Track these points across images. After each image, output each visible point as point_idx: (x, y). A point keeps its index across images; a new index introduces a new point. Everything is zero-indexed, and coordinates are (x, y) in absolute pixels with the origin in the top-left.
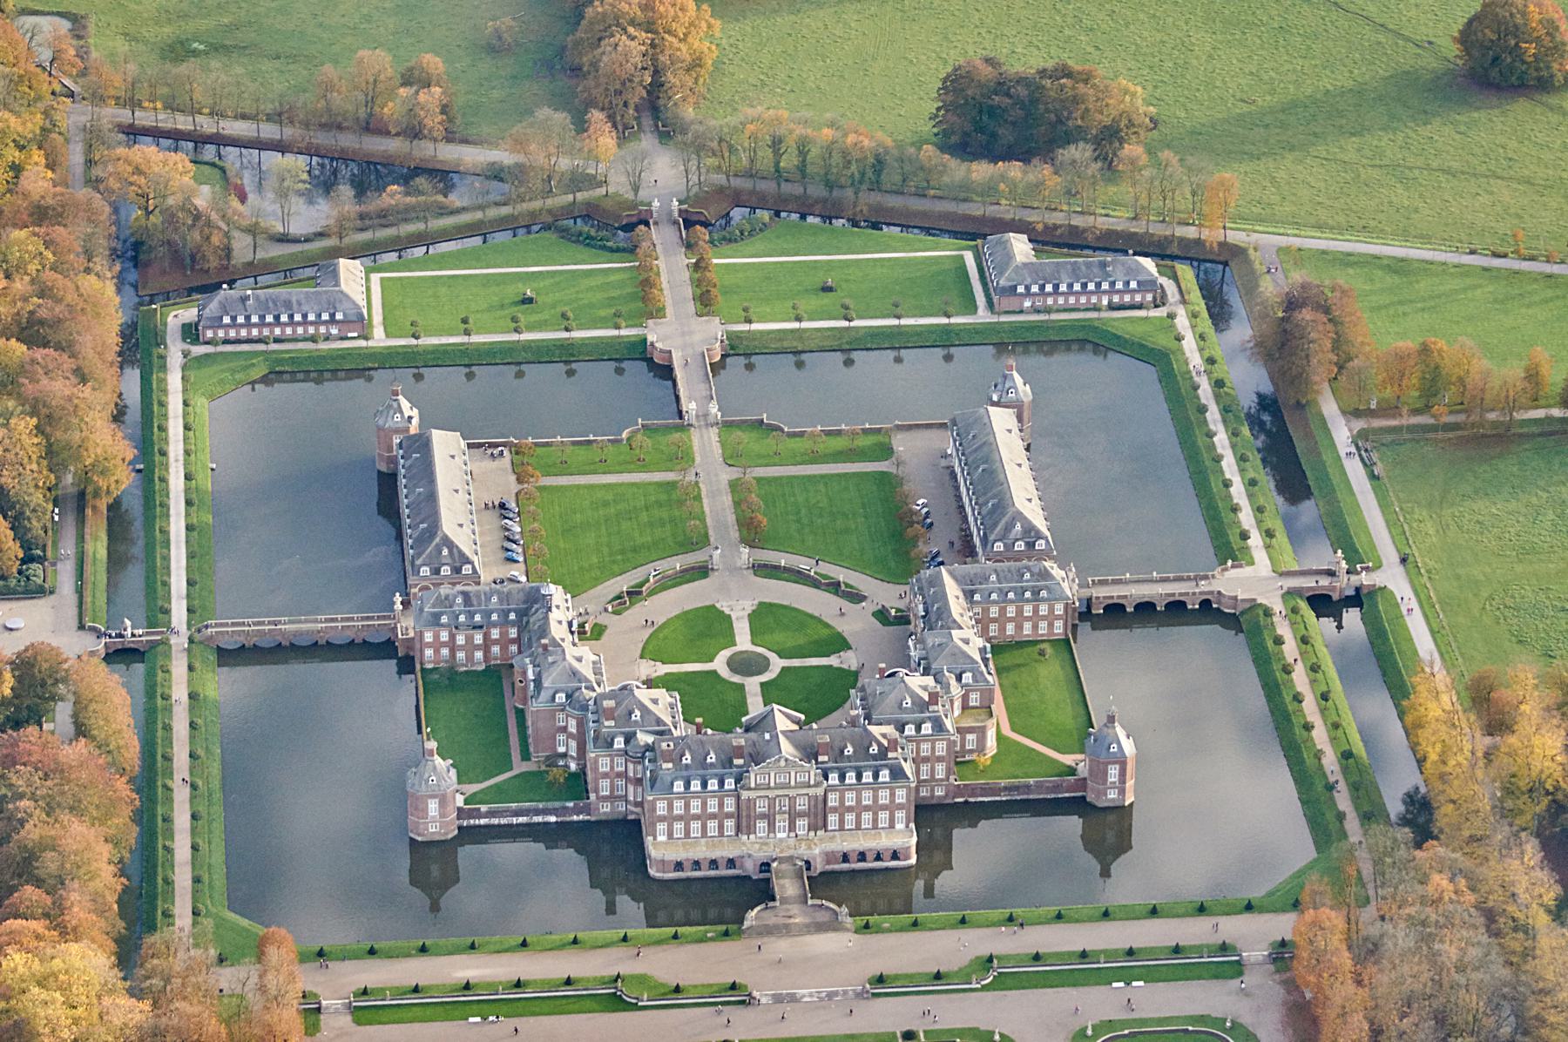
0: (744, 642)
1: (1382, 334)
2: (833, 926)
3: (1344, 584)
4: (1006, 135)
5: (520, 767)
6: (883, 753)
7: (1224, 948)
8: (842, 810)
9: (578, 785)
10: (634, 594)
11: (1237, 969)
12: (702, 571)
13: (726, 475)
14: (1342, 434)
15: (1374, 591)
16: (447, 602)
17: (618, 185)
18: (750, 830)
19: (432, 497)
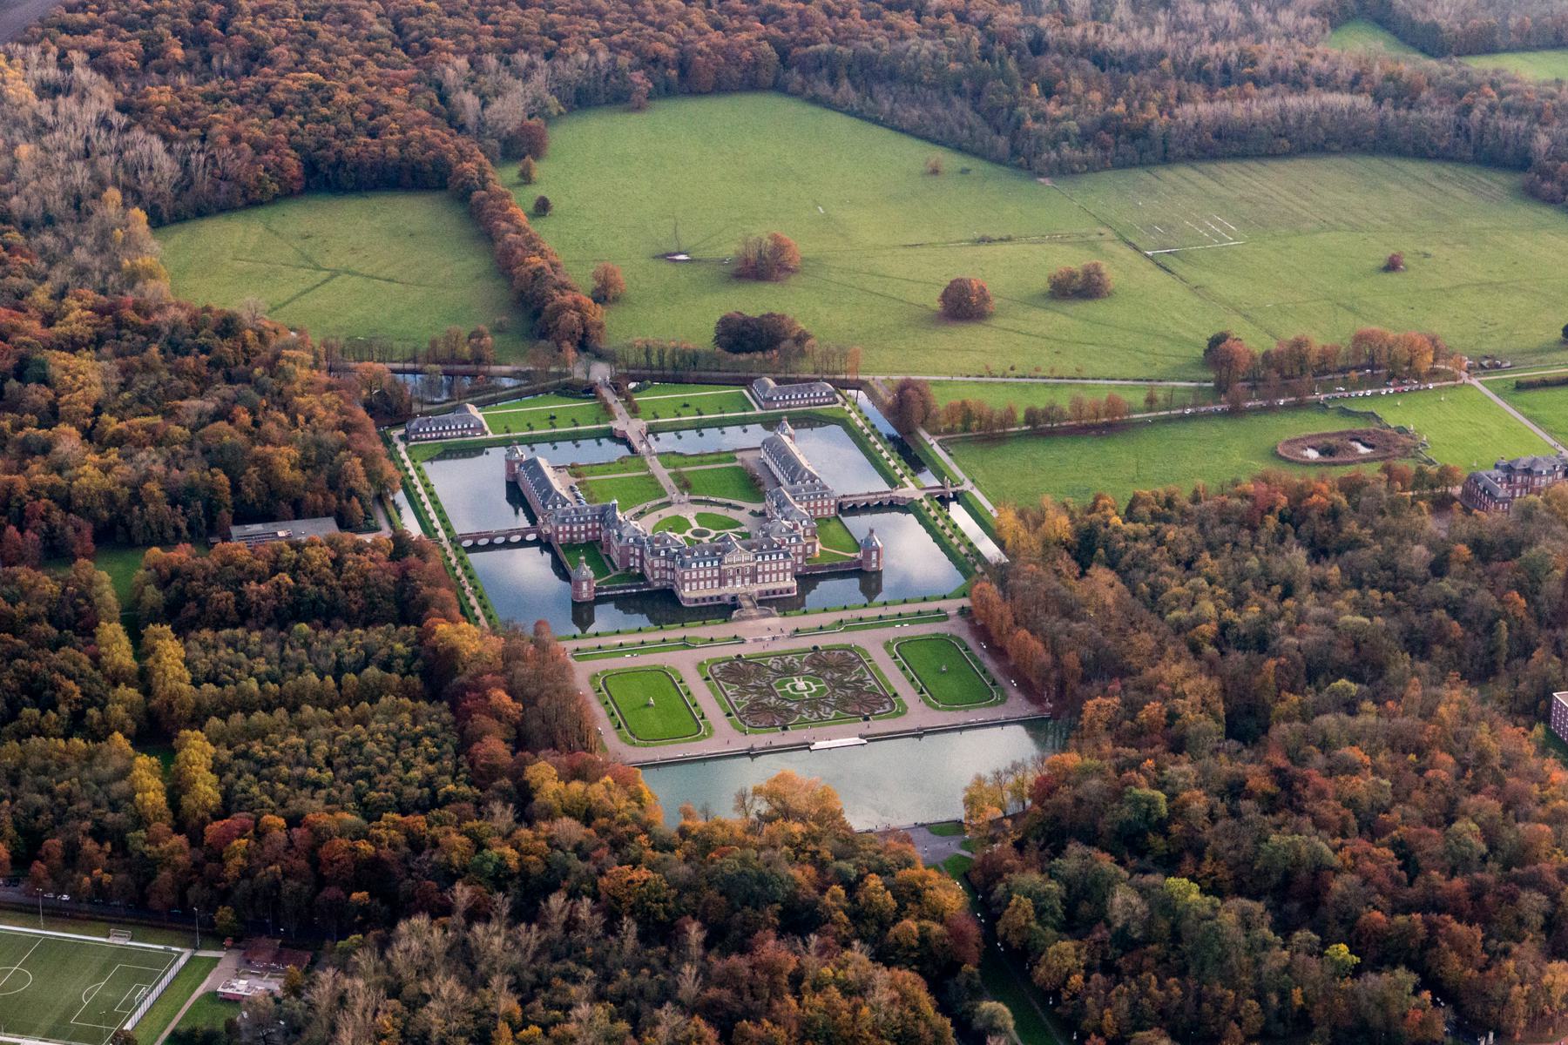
0: (696, 526)
1: (942, 400)
2: (771, 615)
3: (950, 491)
4: (750, 344)
5: (614, 573)
6: (780, 547)
7: (938, 611)
8: (764, 573)
9: (642, 576)
10: (642, 513)
11: (946, 618)
12: (669, 504)
13: (666, 472)
14: (932, 441)
15: (962, 493)
16: (568, 513)
17: (578, 373)
18: (725, 584)
19: (545, 480)
